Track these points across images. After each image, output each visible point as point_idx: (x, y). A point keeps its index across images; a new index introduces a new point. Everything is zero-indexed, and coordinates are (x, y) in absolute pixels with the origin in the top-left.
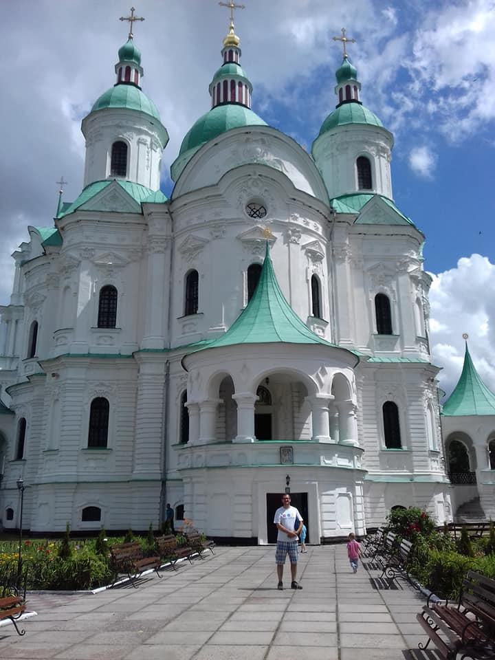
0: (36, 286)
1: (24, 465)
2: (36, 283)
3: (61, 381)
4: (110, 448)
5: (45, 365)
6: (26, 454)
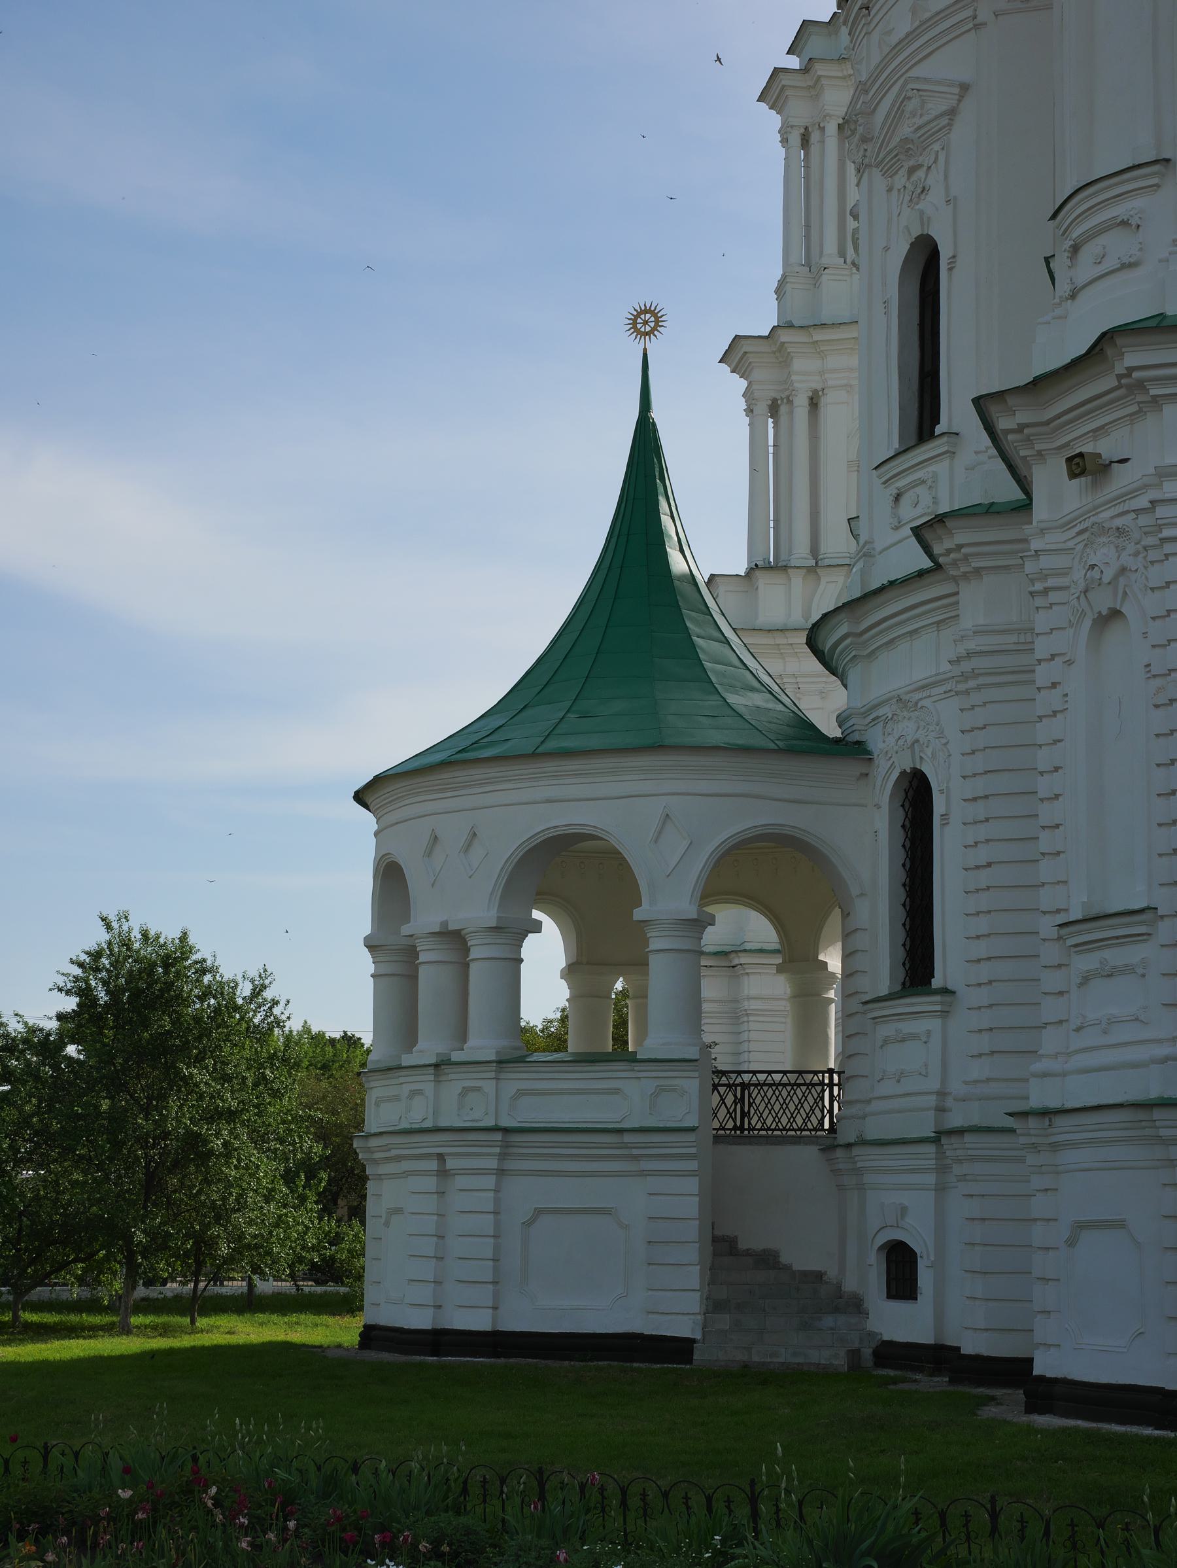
0: (911, 36)
1: (945, 1014)
2: (904, 27)
3: (1134, 493)
5: (1022, 417)
6: (948, 966)
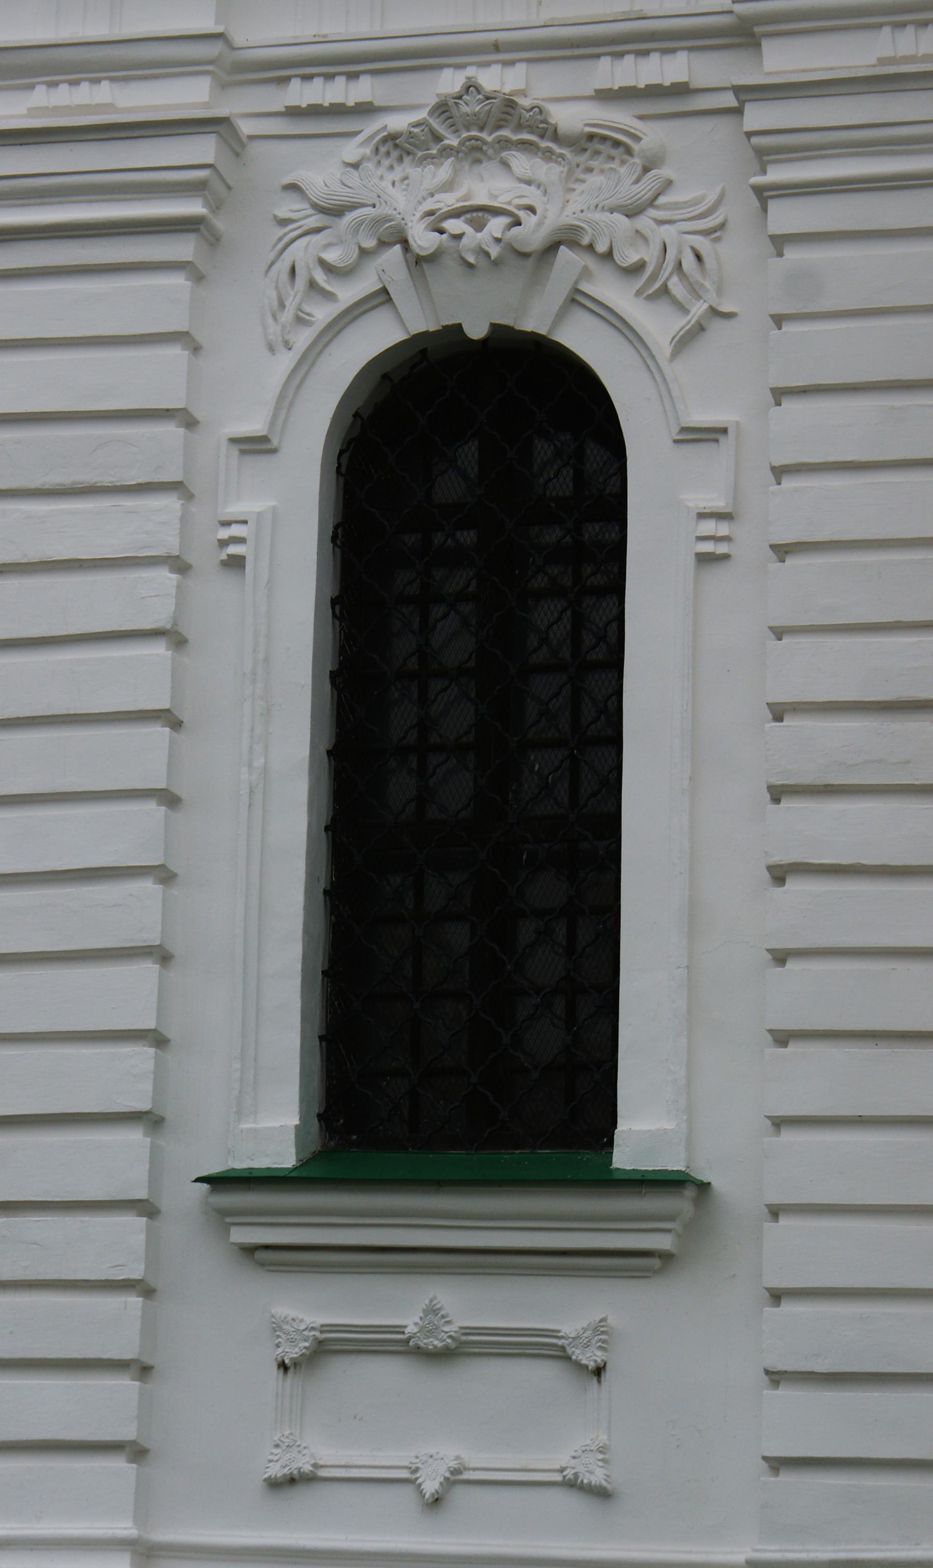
4: (672, 1162)
